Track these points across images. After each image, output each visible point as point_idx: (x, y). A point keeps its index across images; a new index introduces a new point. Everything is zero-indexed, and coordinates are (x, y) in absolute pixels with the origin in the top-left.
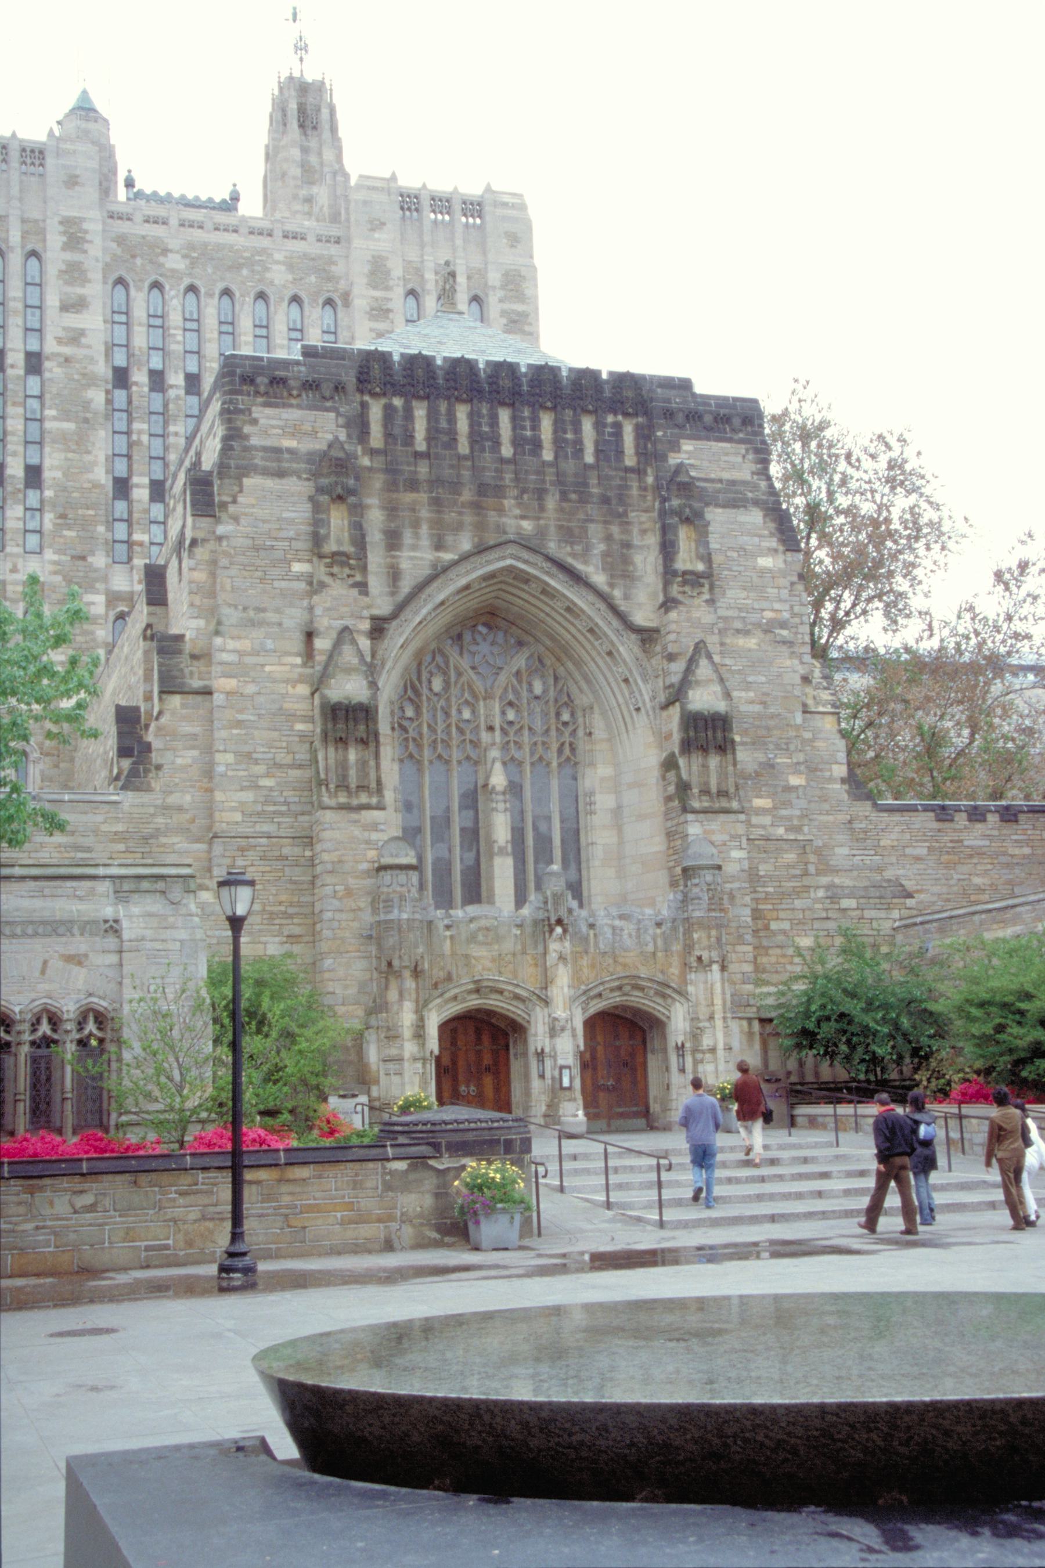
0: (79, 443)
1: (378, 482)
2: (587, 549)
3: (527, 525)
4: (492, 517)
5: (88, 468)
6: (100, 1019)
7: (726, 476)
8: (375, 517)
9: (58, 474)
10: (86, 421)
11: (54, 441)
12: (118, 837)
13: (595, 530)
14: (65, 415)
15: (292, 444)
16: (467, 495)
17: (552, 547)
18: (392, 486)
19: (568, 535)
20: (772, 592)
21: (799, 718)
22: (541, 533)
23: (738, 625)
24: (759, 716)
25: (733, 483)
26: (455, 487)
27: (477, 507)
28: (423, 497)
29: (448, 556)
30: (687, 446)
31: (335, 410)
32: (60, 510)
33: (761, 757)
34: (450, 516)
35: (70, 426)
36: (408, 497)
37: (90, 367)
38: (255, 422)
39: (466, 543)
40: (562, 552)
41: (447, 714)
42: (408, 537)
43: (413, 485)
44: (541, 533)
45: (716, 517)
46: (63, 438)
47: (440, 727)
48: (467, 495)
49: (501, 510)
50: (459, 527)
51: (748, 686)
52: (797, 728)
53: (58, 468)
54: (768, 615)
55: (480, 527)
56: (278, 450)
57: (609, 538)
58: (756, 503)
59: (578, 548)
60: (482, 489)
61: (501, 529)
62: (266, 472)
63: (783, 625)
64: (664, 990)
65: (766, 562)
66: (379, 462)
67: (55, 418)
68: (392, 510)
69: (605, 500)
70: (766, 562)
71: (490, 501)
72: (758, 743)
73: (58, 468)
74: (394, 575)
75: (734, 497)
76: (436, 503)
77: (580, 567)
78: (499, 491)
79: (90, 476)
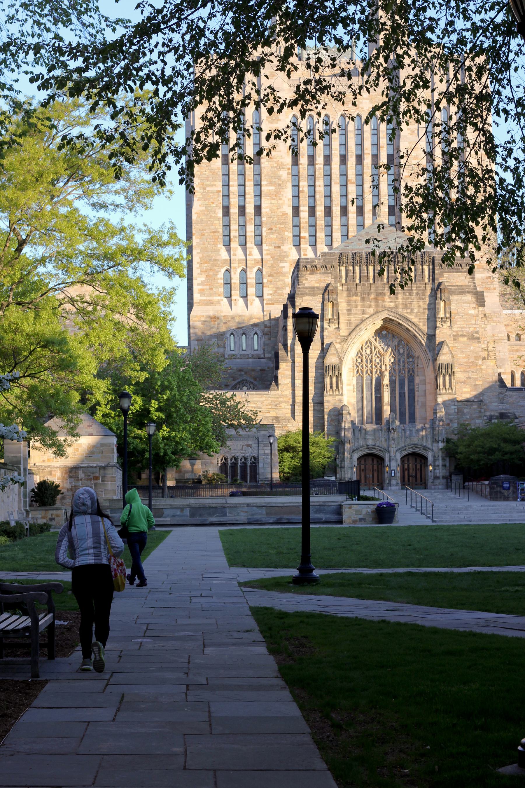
0: (276, 195)
1: (345, 294)
2: (412, 310)
3: (392, 304)
4: (380, 302)
5: (279, 207)
6: (255, 458)
7: (459, 284)
8: (343, 306)
9: (268, 210)
10: (280, 185)
11: (266, 196)
12: (268, 404)
13: (415, 304)
14: (271, 183)
15: (318, 285)
16: (373, 296)
17: (400, 311)
18: (349, 295)
19: (406, 306)
20: (473, 322)
21: (480, 362)
22: (397, 306)
23: (460, 333)
24: (466, 362)
25: (461, 286)
26: (369, 294)
27: (376, 299)
28: (359, 298)
29: (366, 316)
30: (446, 275)
31: (331, 273)
32: (269, 226)
33: (466, 375)
34: (367, 303)
35: (272, 188)
36: (354, 298)
37: (281, 160)
38: (306, 279)
39: (371, 311)
40: (404, 312)
41: (371, 361)
42: (354, 310)
43: (356, 295)
44: (397, 306)
45: (454, 299)
46: (270, 194)
47: (369, 366)
48: (373, 296)
49: (384, 300)
50: (370, 306)
51: (463, 353)
52: (480, 366)
53: (267, 207)
54: (472, 329)
55: (377, 306)
56: (313, 288)
57: (419, 306)
58: (469, 292)
59: (409, 311)
60: (378, 294)
61: (384, 306)
62: (310, 295)
63: (477, 332)
64: (425, 448)
65: (472, 312)
66: (345, 288)
67: (266, 185)
68: (349, 303)
69: (418, 294)
70: (472, 312)
71: (380, 297)
72: (465, 371)
73: (267, 207)
74: (349, 323)
75: (461, 291)
76: (363, 299)
77: (409, 317)
78: (383, 294)
79: (282, 210)
